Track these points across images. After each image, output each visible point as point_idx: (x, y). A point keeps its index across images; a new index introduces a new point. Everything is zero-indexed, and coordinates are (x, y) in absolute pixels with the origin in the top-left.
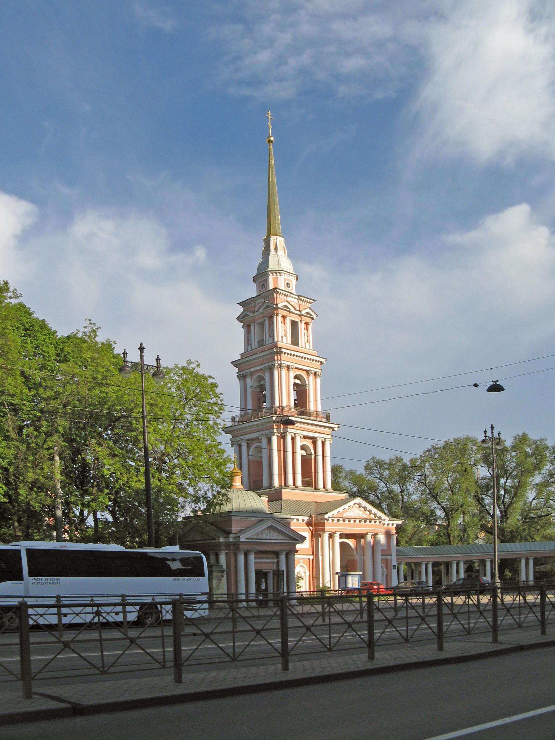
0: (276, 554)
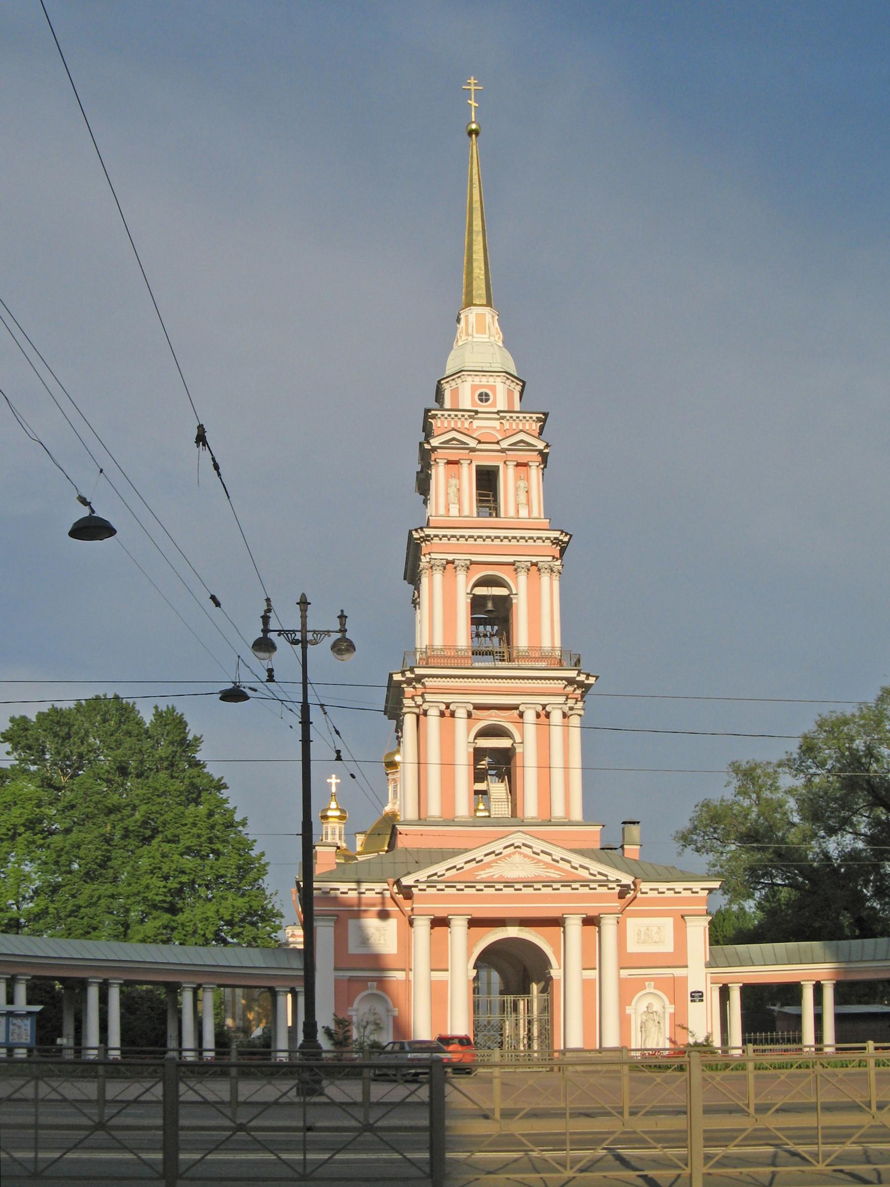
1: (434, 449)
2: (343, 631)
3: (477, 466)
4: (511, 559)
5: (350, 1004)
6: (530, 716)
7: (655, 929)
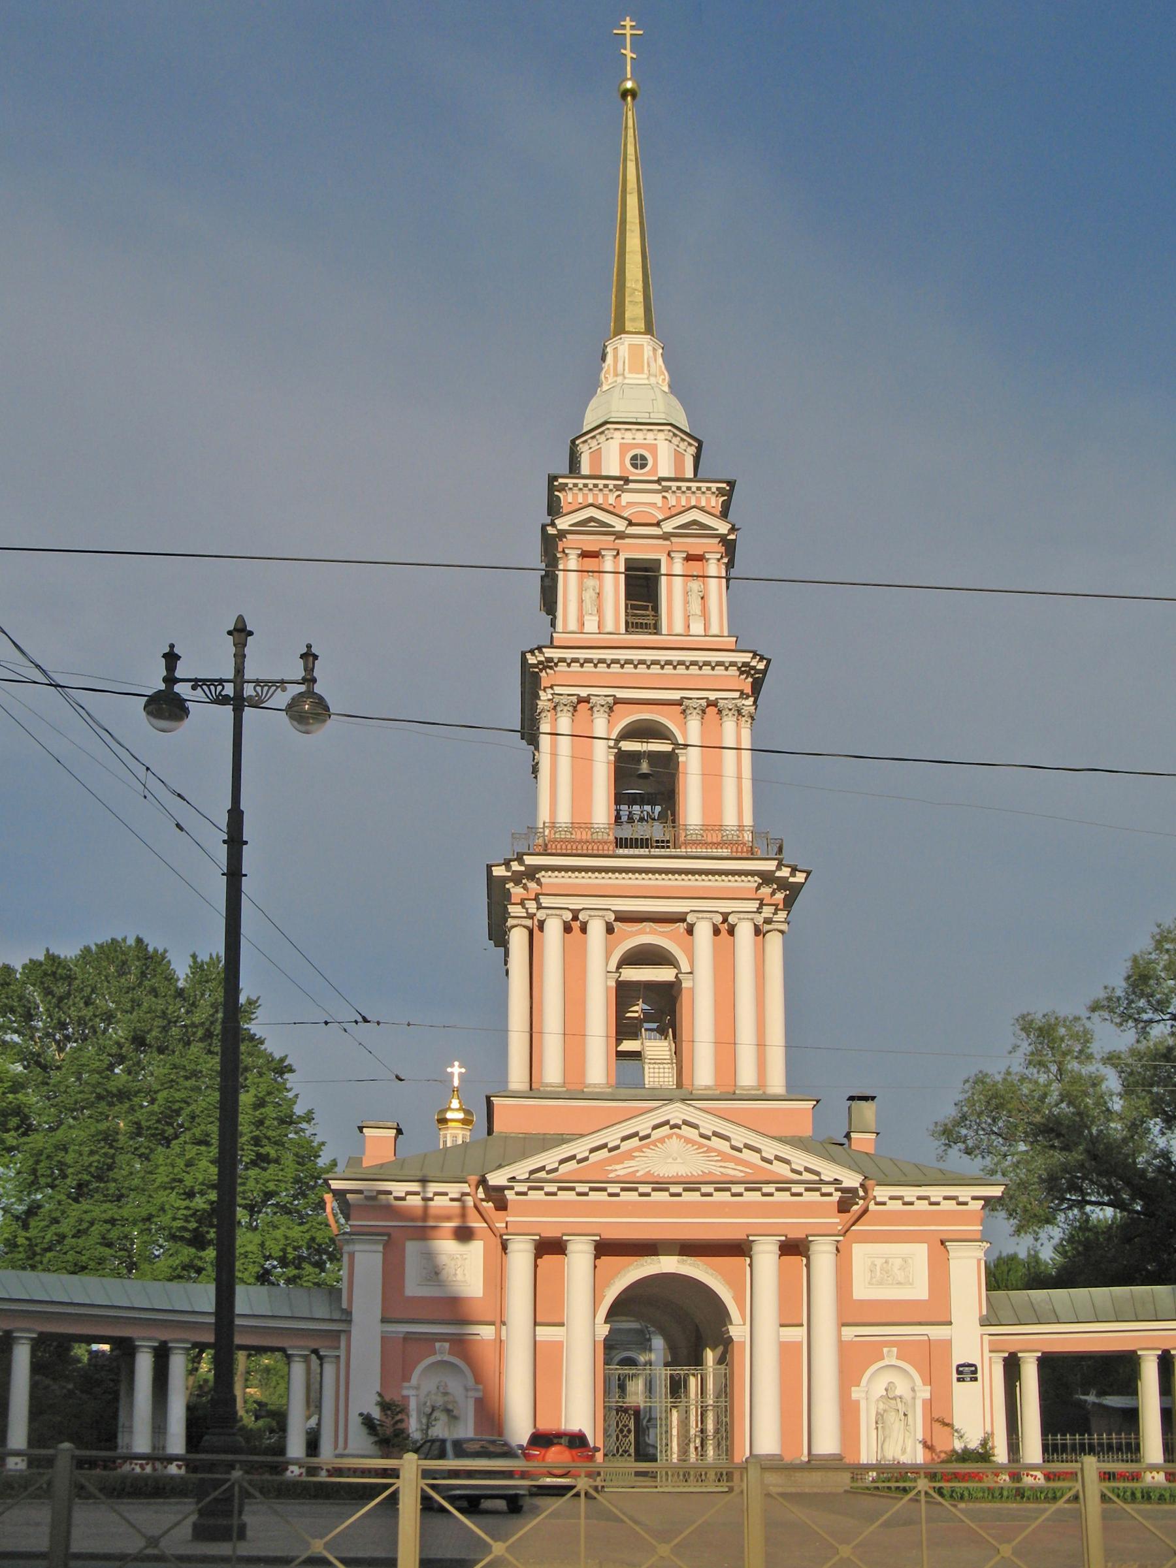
1: (562, 534)
2: (309, 680)
3: (626, 559)
4: (676, 695)
5: (406, 1378)
6: (703, 930)
7: (898, 1262)
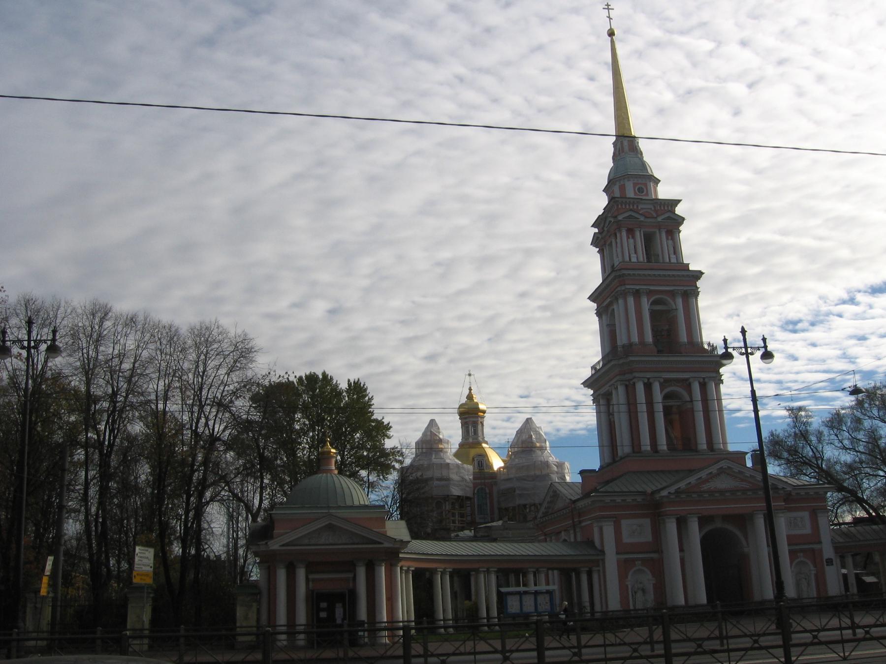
0: (350, 566)
2: (765, 347)
